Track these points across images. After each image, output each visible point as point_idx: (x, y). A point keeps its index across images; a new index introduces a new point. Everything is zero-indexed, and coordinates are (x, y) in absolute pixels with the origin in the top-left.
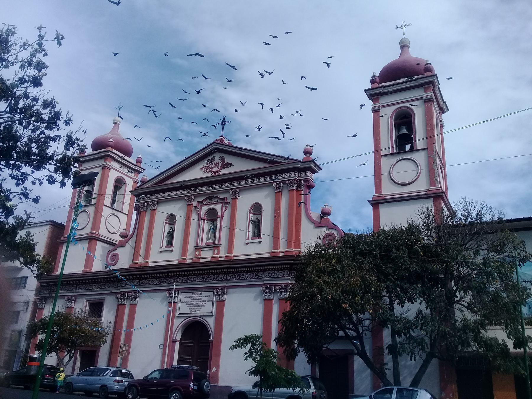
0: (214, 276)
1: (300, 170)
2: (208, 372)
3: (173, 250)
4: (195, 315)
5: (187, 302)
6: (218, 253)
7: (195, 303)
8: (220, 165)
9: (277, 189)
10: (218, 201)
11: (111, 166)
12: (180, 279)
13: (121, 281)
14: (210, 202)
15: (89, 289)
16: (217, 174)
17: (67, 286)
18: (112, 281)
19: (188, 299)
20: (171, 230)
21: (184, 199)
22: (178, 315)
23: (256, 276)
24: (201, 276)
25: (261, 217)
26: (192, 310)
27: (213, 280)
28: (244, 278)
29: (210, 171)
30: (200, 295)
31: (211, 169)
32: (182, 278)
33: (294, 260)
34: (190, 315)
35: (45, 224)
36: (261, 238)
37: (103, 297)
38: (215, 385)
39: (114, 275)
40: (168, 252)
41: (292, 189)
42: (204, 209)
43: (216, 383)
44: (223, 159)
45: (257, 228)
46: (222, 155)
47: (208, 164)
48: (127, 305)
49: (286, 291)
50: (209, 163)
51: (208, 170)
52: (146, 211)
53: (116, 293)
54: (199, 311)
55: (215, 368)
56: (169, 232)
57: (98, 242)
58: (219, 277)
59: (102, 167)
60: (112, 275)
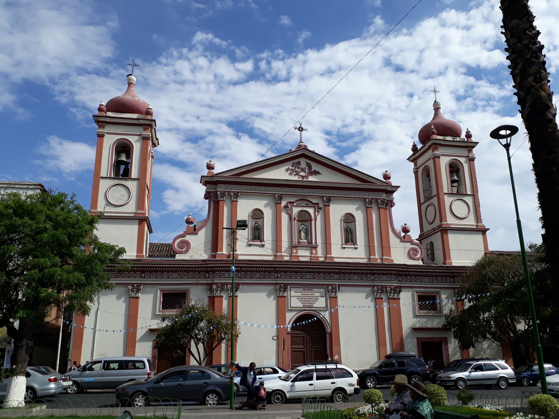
0: (325, 275)
4: (309, 309)
5: (298, 296)
7: (307, 298)
13: (210, 272)
18: (198, 271)
19: (299, 294)
26: (305, 304)
32: (290, 274)
33: (403, 268)
34: (303, 309)
36: (357, 245)
45: (350, 235)
48: (224, 297)
53: (207, 284)
60: (203, 266)
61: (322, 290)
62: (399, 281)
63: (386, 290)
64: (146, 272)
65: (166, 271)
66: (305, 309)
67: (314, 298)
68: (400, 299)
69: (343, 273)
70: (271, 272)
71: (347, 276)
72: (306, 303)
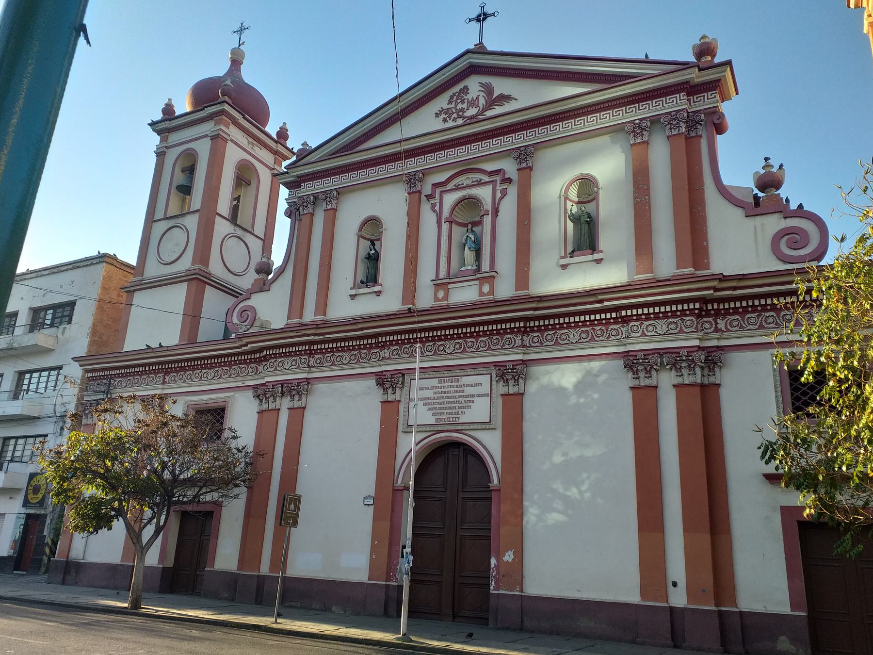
1: (692, 90)
2: (493, 561)
3: (380, 292)
5: (426, 399)
6: (492, 291)
8: (482, 101)
9: (635, 136)
10: (481, 180)
11: (229, 135)
12: (406, 350)
14: (463, 184)
15: (192, 380)
16: (475, 120)
17: (145, 376)
19: (429, 393)
20: (373, 252)
21: (401, 181)
22: (406, 430)
23: (602, 336)
24: (457, 341)
25: (595, 206)
27: (489, 349)
28: (568, 340)
29: (458, 118)
30: (458, 384)
31: (461, 113)
33: (716, 289)
34: (436, 429)
35: (95, 262)
36: (601, 252)
37: (225, 398)
38: (514, 593)
39: (249, 346)
40: (369, 296)
41: (677, 132)
42: (450, 199)
43: (518, 589)
44: (488, 89)
46: (485, 79)
47: (454, 102)
49: (692, 366)
50: (456, 102)
51: (455, 115)
52: (312, 214)
54: (458, 418)
55: (510, 553)
56: (369, 254)
57: (208, 287)
58: (502, 339)
59: (210, 137)
60: (243, 348)
61: (485, 380)
62: (717, 330)
63: (662, 363)
64: (171, 373)
65: (198, 369)
66: (440, 428)
67: (462, 400)
68: (719, 385)
69: (539, 329)
70: (371, 348)
71: (550, 337)
72: (442, 414)
